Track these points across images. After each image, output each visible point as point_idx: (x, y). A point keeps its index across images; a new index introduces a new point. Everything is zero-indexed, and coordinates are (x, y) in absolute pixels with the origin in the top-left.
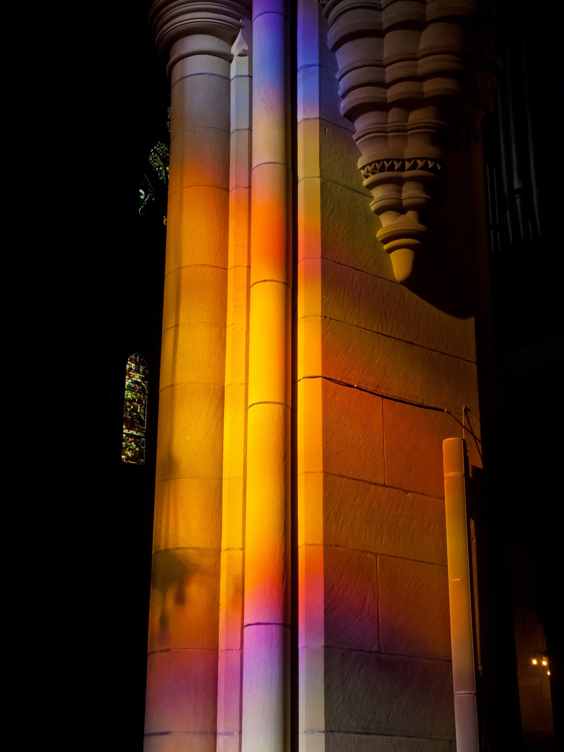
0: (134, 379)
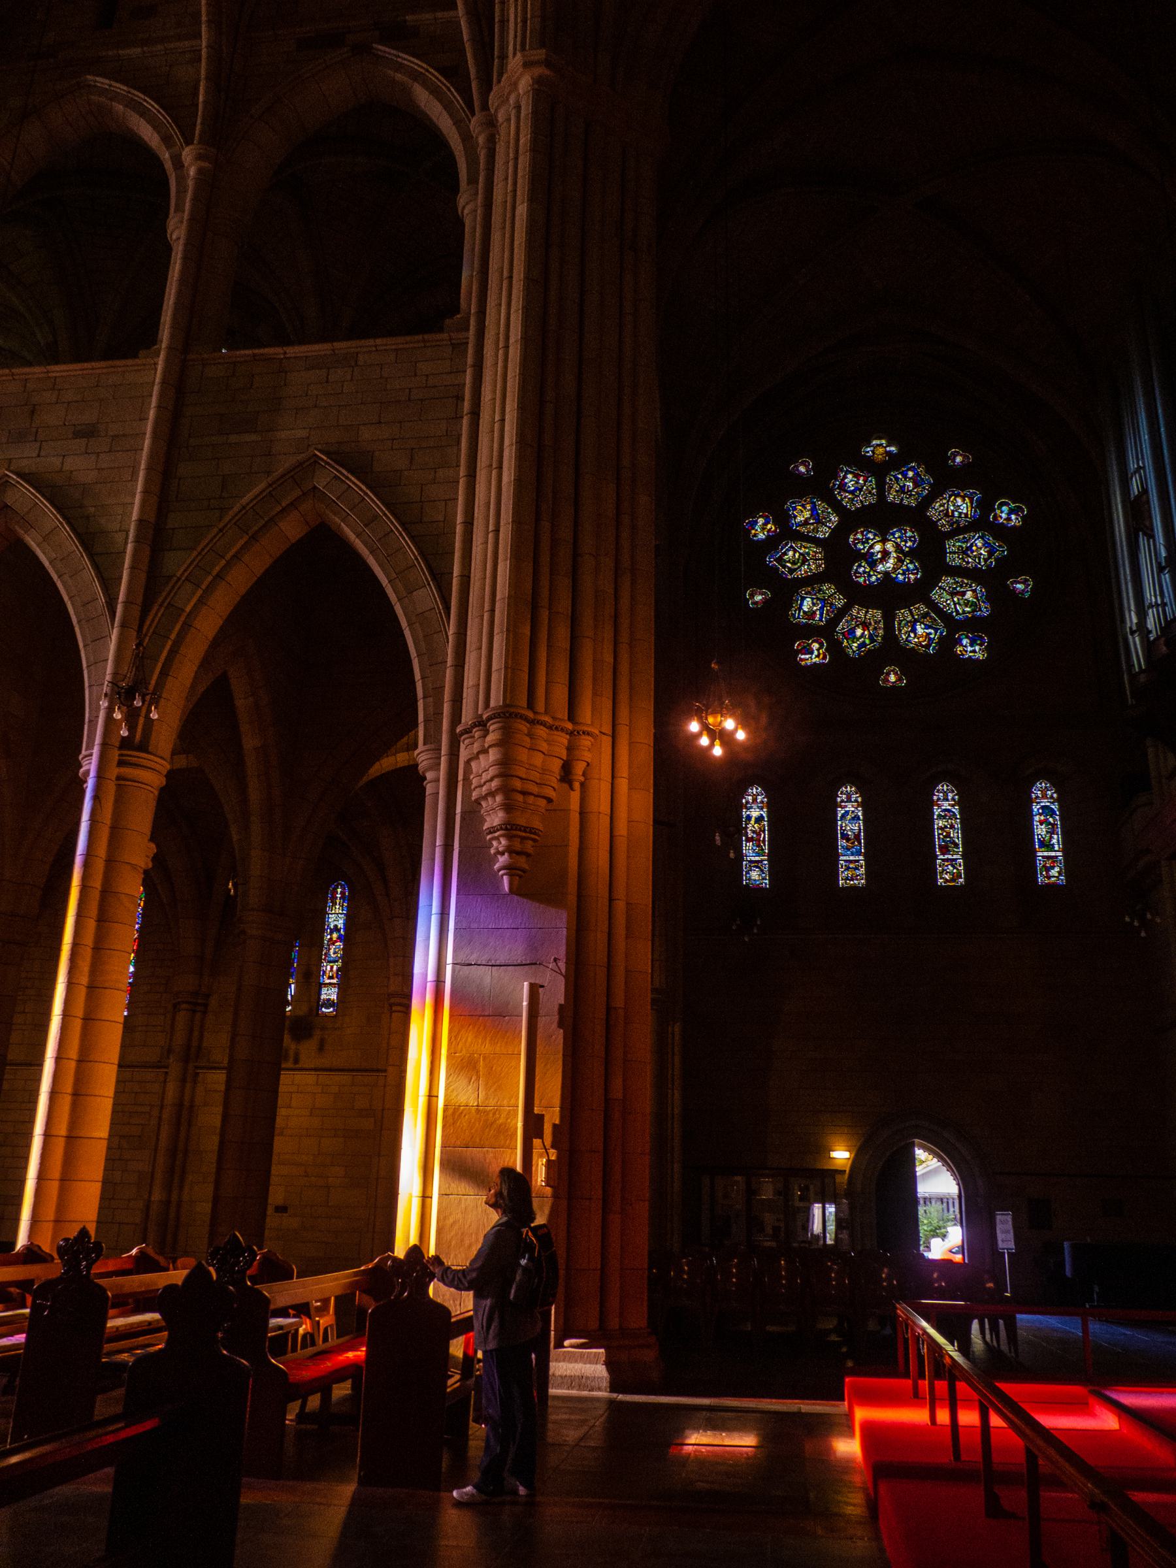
0: (943, 808)
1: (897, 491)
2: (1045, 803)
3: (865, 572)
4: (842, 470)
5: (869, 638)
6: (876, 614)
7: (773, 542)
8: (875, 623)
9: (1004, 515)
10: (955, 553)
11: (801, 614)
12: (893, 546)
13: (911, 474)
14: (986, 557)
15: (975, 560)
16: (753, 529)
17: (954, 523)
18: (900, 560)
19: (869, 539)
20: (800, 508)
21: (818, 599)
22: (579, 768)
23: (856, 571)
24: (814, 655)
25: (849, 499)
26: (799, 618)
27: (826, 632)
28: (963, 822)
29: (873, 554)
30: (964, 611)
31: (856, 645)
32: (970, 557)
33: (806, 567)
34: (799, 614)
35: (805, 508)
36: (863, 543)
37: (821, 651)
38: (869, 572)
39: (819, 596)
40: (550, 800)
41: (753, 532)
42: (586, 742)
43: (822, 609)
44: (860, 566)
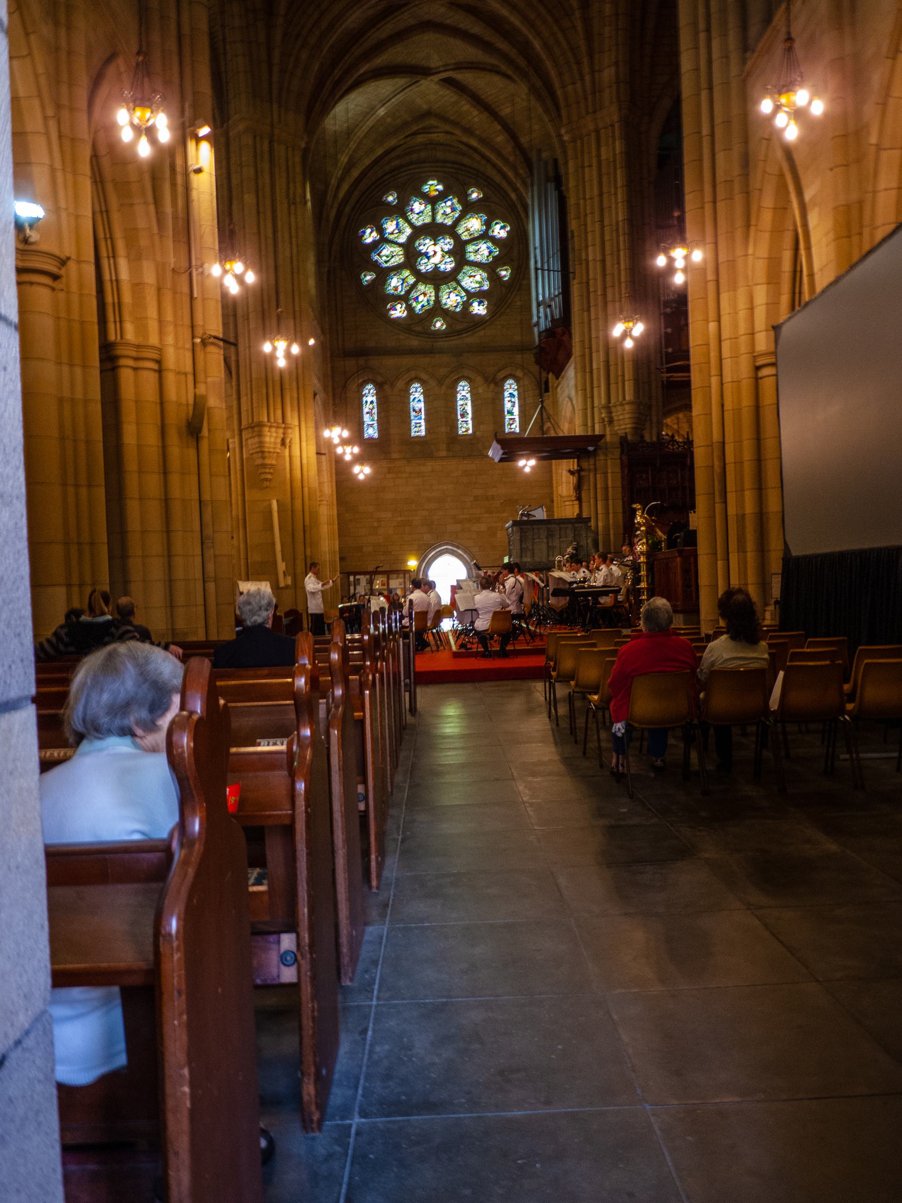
2: (511, 391)
6: (430, 290)
7: (376, 245)
18: (443, 256)
22: (288, 441)
24: (399, 312)
27: (404, 298)
28: (472, 402)
39: (401, 277)
40: (278, 453)
42: (290, 431)
43: (402, 284)
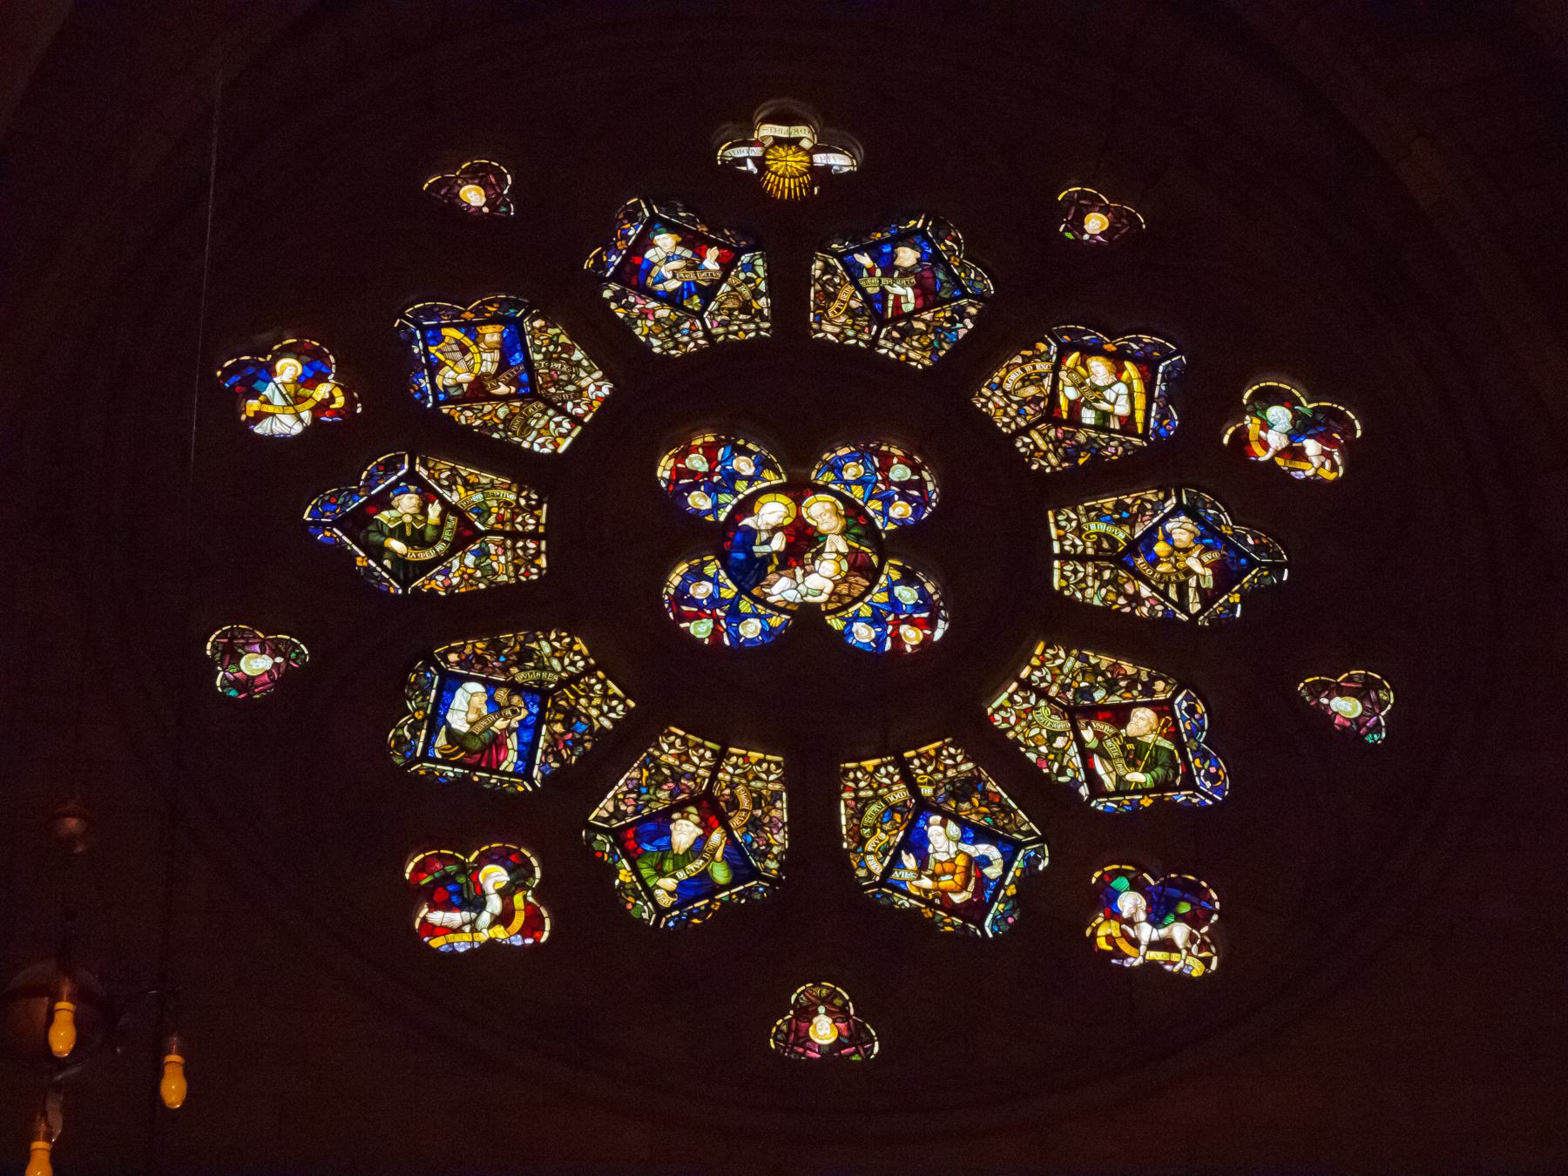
1: (851, 312)
3: (715, 601)
4: (632, 217)
5: (727, 858)
8: (756, 803)
9: (1277, 440)
10: (1083, 558)
11: (441, 741)
12: (837, 513)
13: (907, 257)
14: (1209, 583)
15: (1165, 594)
16: (256, 395)
17: (1080, 447)
18: (858, 566)
19: (734, 476)
20: (451, 333)
21: (515, 688)
23: (682, 594)
25: (658, 321)
26: (425, 757)
29: (751, 533)
30: (1120, 779)
31: (669, 883)
32: (1147, 582)
33: (470, 560)
34: (429, 743)
35: (476, 338)
36: (712, 490)
37: (518, 900)
38: (734, 602)
39: (520, 678)
41: (253, 406)
43: (530, 729)
44: (697, 575)
